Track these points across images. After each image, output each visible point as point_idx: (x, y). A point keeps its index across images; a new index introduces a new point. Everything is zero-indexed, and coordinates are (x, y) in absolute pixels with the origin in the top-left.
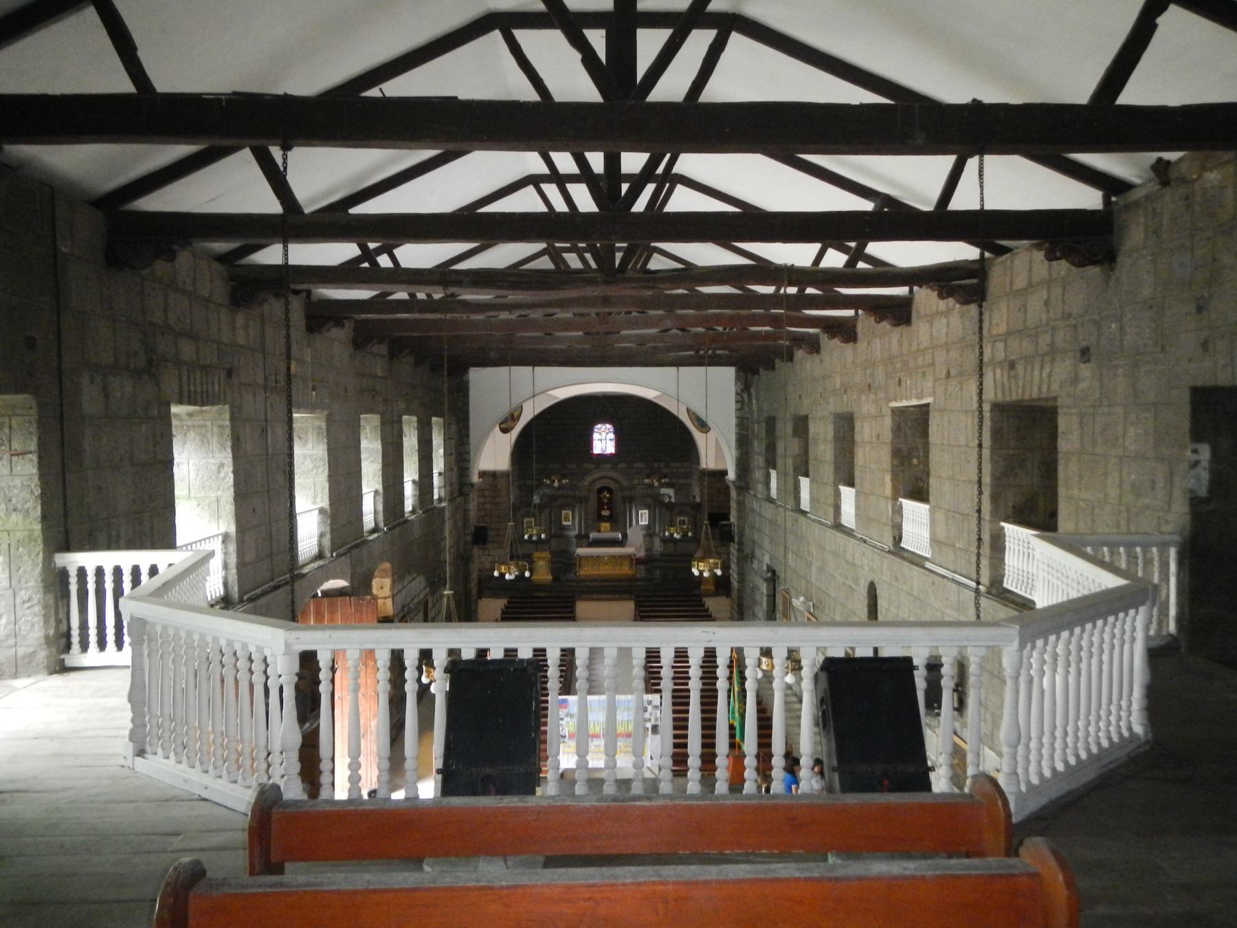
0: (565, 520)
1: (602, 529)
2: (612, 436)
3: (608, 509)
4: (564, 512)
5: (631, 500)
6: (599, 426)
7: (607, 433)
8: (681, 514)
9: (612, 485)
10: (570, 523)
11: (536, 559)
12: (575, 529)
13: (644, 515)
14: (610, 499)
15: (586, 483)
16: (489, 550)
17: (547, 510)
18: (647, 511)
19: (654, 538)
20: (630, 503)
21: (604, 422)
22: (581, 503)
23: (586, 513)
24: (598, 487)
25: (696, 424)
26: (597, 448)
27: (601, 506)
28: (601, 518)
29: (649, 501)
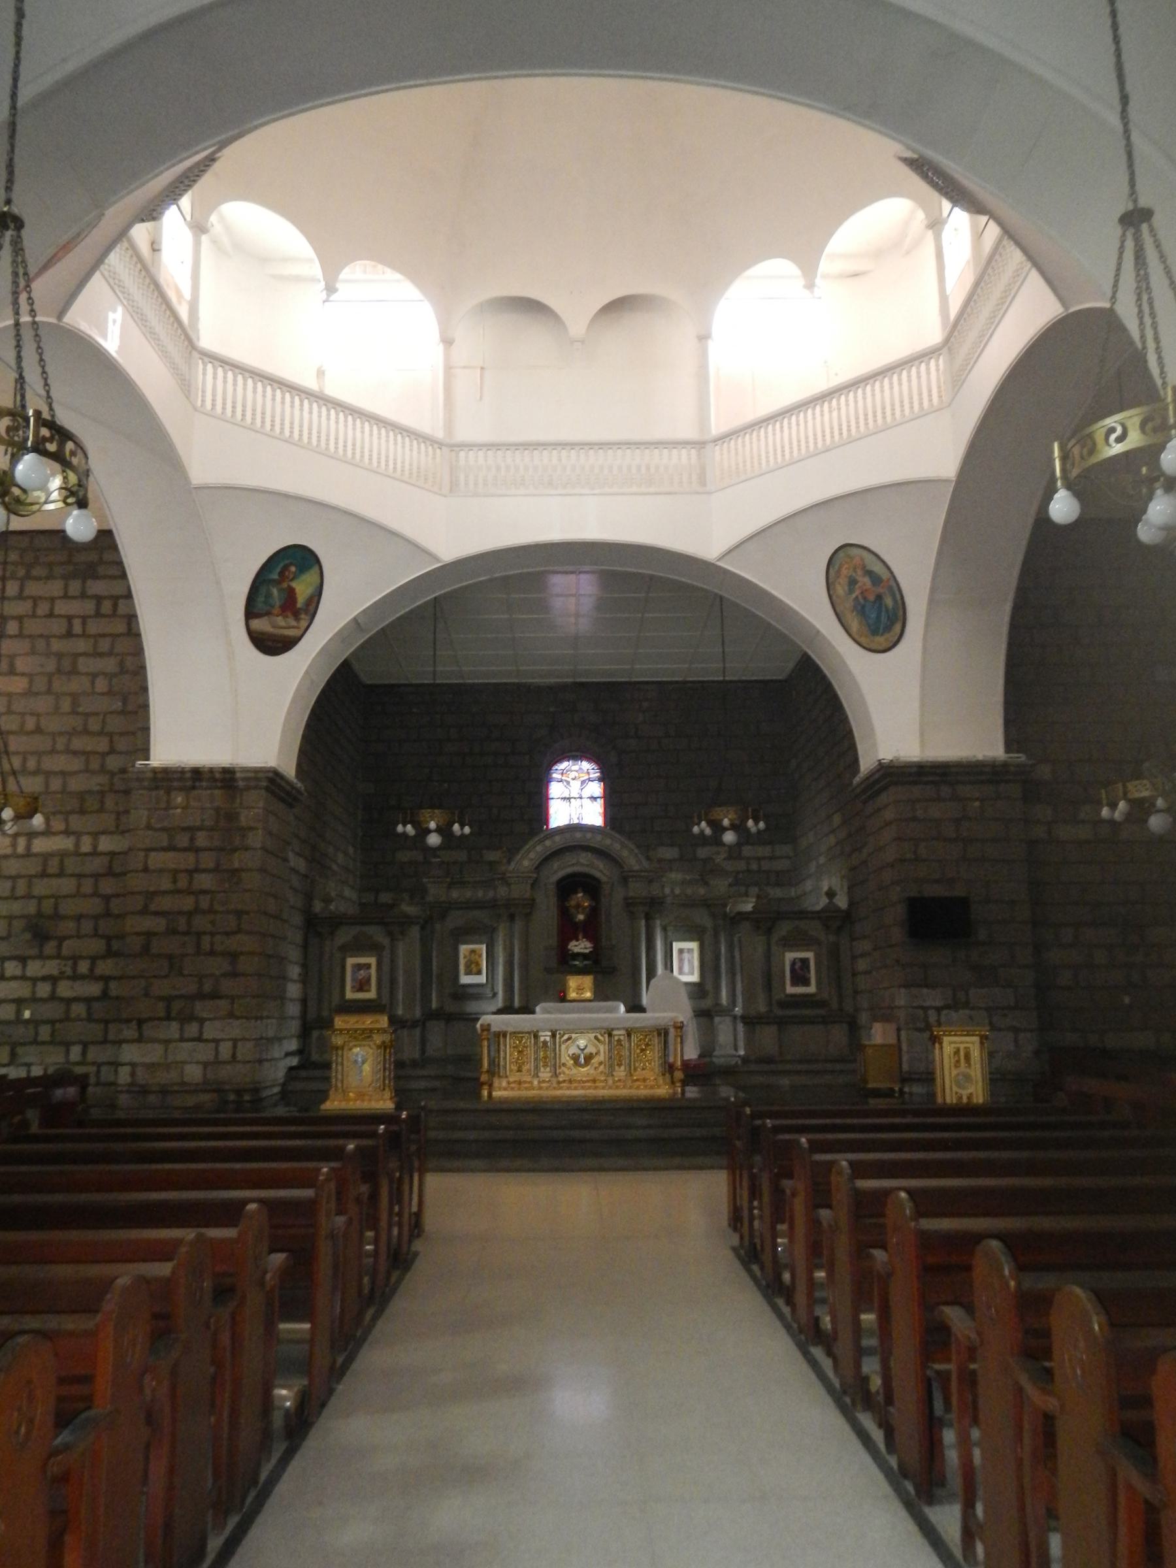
0: (469, 972)
1: (573, 995)
2: (596, 789)
3: (587, 937)
4: (464, 949)
5: (652, 907)
6: (564, 765)
7: (583, 782)
8: (790, 943)
9: (600, 870)
10: (482, 979)
11: (338, 1040)
12: (495, 995)
13: (686, 956)
14: (594, 913)
15: (526, 863)
16: (202, 1021)
17: (415, 932)
18: (694, 945)
19: (717, 1019)
20: (648, 918)
21: (576, 755)
22: (512, 918)
23: (526, 950)
24: (561, 874)
25: (855, 625)
26: (560, 815)
27: (568, 929)
28: (566, 963)
29: (703, 918)
